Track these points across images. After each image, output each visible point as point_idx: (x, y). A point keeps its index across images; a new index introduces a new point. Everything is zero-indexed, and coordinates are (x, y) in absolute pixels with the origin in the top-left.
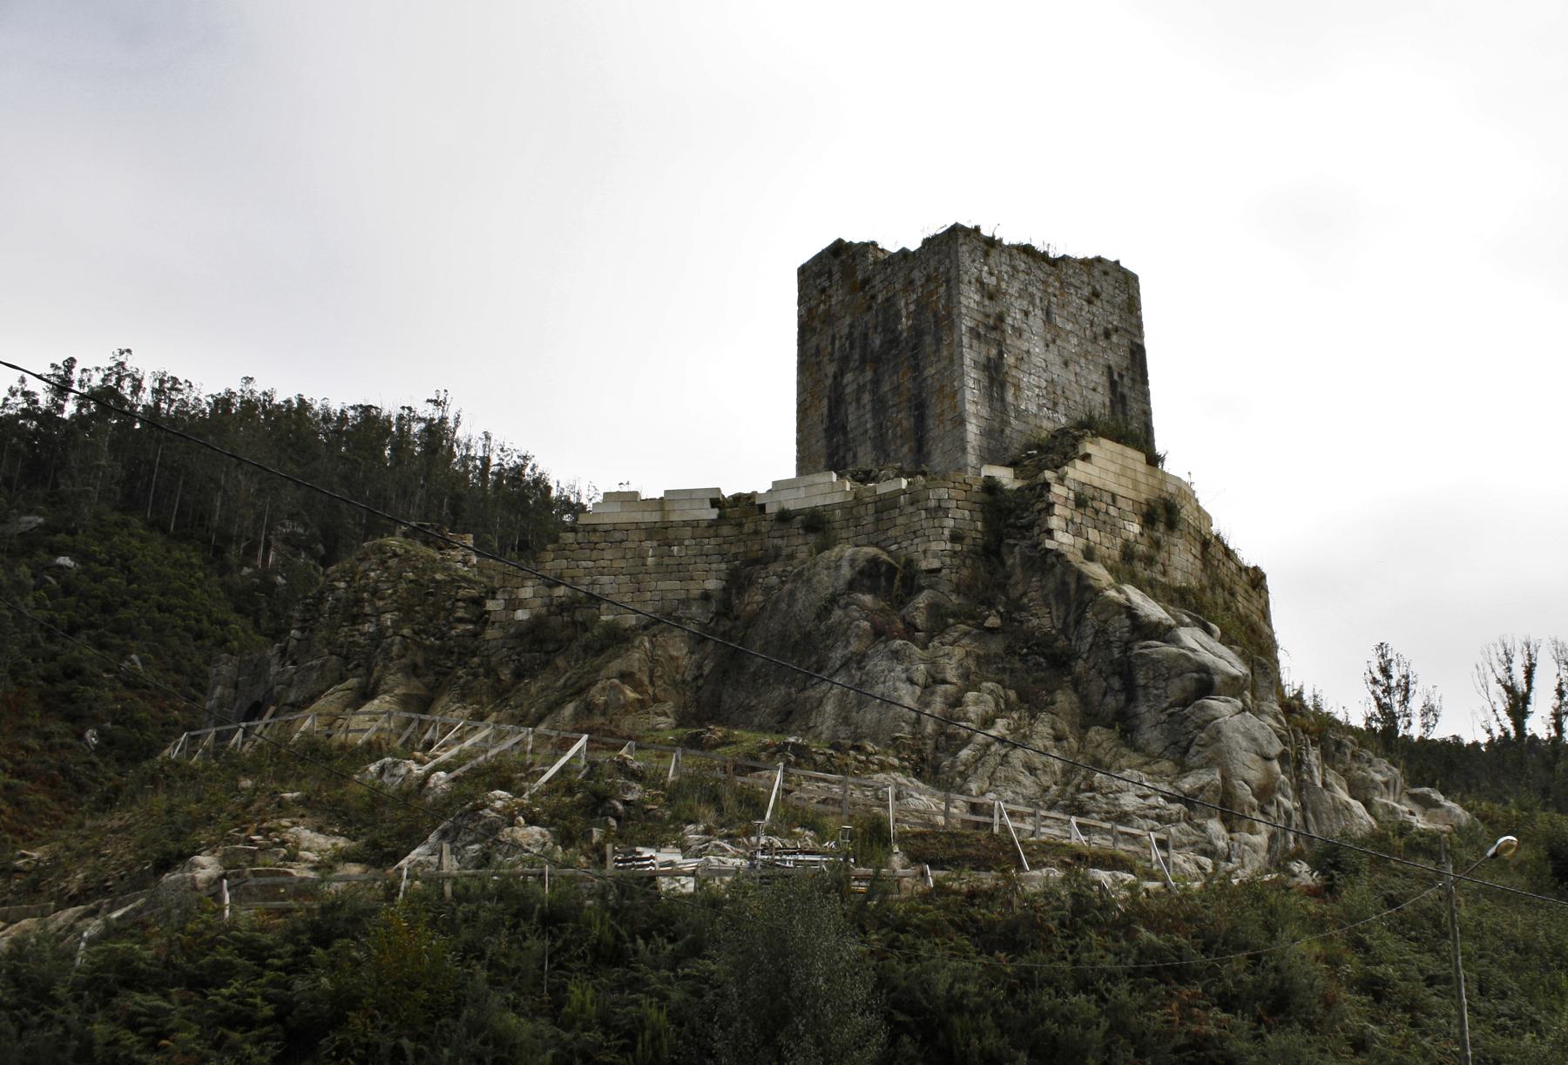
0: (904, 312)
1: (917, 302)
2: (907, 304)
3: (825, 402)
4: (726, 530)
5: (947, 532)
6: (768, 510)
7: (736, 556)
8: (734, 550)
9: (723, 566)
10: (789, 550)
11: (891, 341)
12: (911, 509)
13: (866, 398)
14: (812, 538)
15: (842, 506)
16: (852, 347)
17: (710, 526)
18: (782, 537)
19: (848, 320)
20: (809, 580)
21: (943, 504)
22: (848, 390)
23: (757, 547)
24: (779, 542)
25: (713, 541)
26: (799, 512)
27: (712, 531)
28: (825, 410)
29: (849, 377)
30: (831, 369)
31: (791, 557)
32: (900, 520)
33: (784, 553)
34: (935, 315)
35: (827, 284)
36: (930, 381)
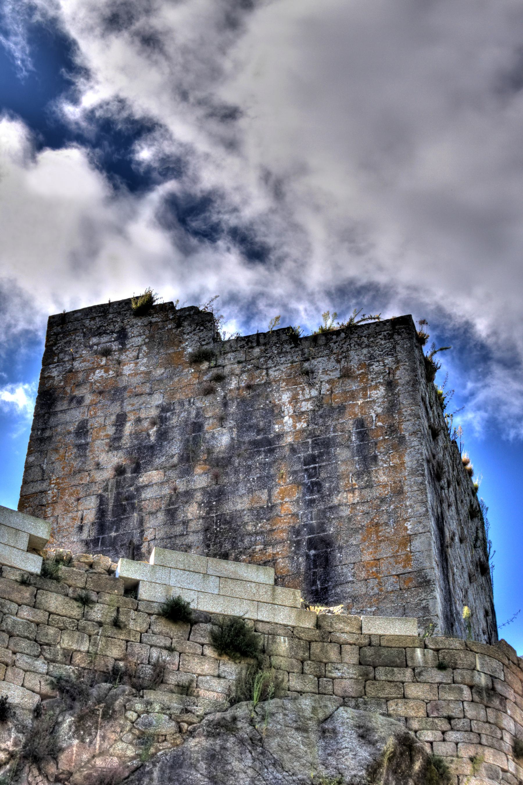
0: (288, 409)
1: (319, 401)
2: (294, 400)
3: (92, 503)
4: (54, 601)
5: (507, 738)
6: (144, 593)
7: (69, 656)
8: (66, 642)
9: (41, 665)
10: (184, 679)
11: (255, 444)
12: (438, 676)
13: (192, 511)
14: (232, 669)
15: (292, 633)
16: (163, 435)
17: (24, 582)
18: (170, 649)
19: (158, 399)
20: (256, 742)
21: (499, 687)
22: (147, 494)
23: (115, 652)
24: (165, 655)
25: (26, 613)
26: (207, 618)
27: (27, 593)
28: (91, 516)
29: (152, 475)
30: (111, 460)
31: (186, 690)
32: (413, 690)
33: (172, 679)
34: (360, 424)
35: (115, 346)
36: (346, 512)
